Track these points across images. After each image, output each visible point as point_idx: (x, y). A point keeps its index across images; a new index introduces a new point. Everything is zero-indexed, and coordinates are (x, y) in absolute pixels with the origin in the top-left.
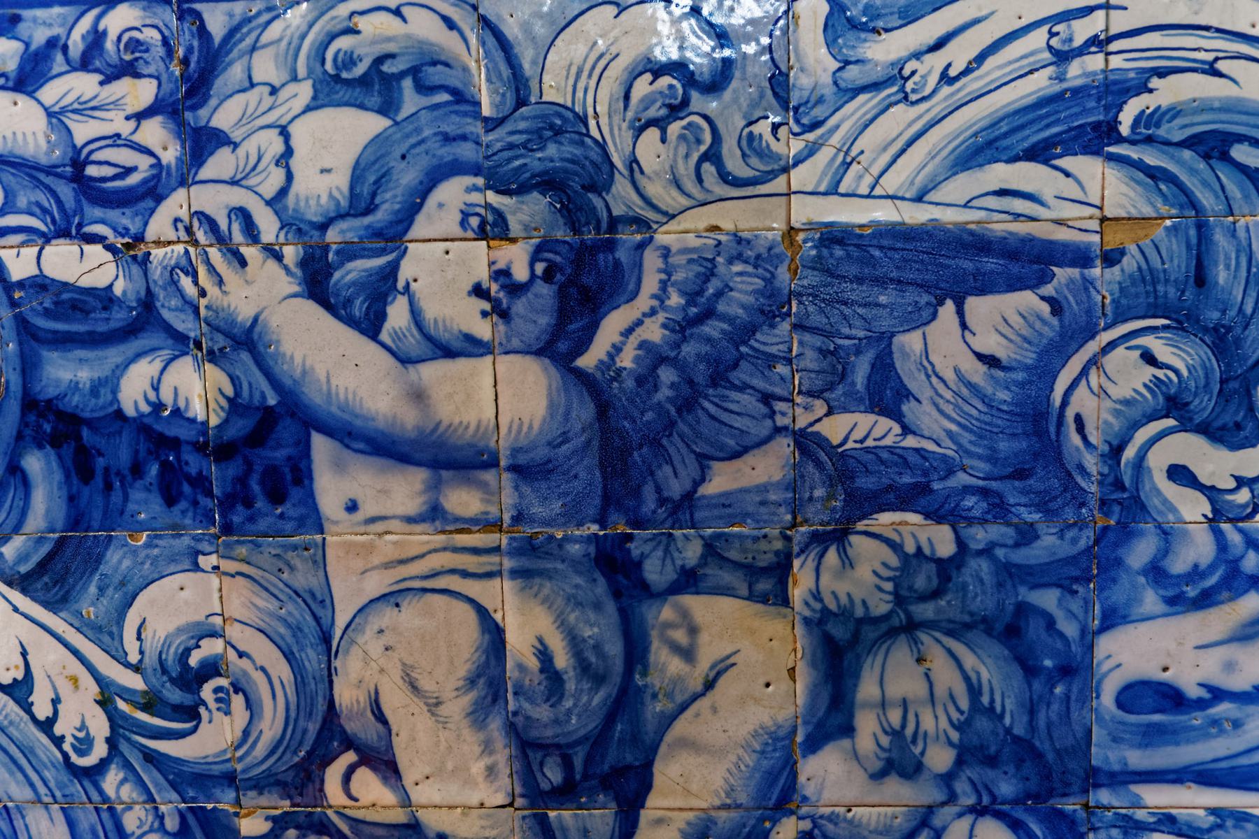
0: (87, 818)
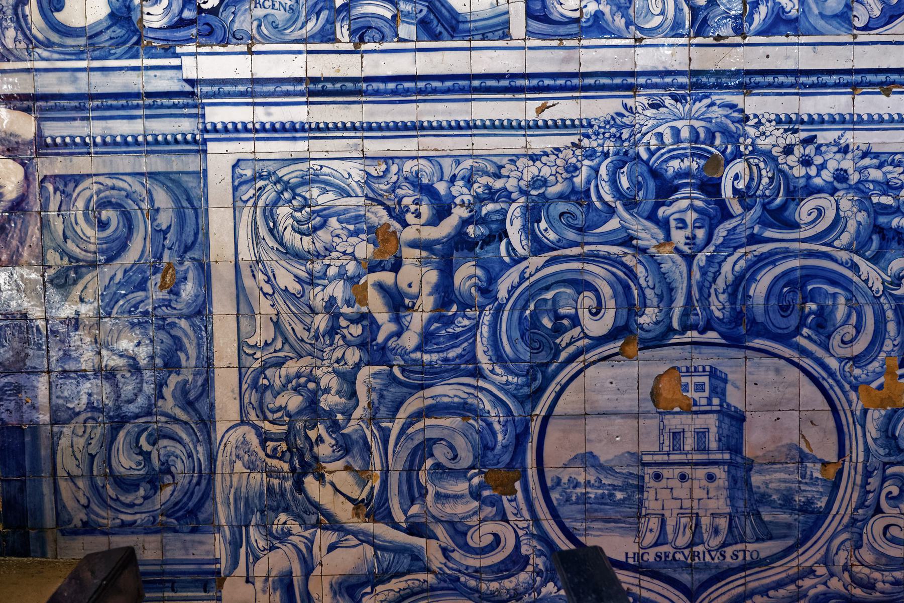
0: (876, 307)
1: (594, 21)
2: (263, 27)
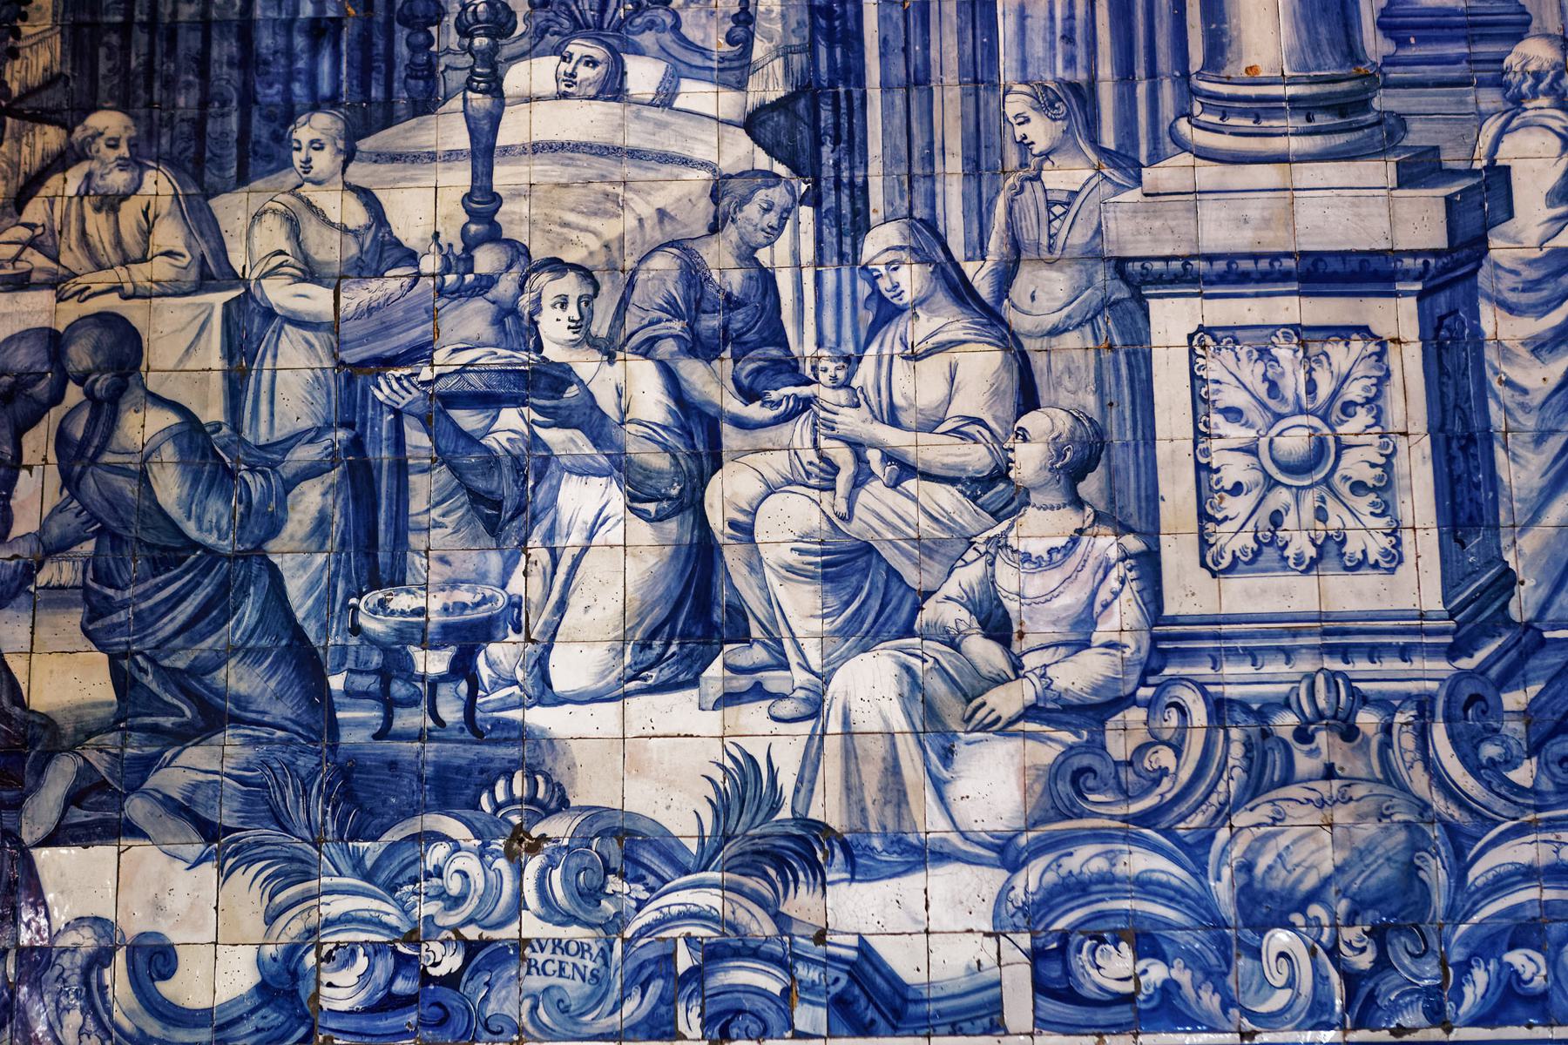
1: (1163, 1000)
2: (541, 1011)
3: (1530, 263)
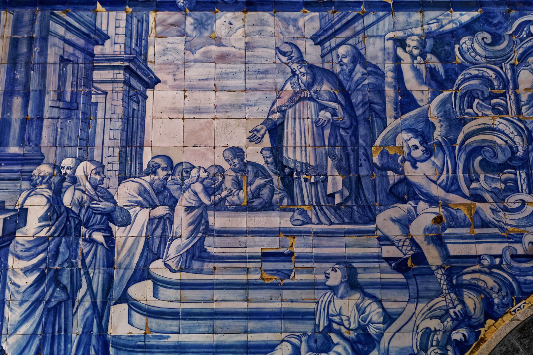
3: (29, 242)
